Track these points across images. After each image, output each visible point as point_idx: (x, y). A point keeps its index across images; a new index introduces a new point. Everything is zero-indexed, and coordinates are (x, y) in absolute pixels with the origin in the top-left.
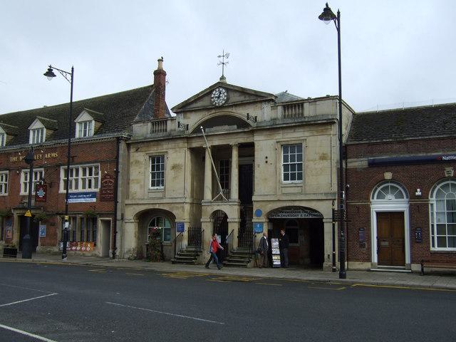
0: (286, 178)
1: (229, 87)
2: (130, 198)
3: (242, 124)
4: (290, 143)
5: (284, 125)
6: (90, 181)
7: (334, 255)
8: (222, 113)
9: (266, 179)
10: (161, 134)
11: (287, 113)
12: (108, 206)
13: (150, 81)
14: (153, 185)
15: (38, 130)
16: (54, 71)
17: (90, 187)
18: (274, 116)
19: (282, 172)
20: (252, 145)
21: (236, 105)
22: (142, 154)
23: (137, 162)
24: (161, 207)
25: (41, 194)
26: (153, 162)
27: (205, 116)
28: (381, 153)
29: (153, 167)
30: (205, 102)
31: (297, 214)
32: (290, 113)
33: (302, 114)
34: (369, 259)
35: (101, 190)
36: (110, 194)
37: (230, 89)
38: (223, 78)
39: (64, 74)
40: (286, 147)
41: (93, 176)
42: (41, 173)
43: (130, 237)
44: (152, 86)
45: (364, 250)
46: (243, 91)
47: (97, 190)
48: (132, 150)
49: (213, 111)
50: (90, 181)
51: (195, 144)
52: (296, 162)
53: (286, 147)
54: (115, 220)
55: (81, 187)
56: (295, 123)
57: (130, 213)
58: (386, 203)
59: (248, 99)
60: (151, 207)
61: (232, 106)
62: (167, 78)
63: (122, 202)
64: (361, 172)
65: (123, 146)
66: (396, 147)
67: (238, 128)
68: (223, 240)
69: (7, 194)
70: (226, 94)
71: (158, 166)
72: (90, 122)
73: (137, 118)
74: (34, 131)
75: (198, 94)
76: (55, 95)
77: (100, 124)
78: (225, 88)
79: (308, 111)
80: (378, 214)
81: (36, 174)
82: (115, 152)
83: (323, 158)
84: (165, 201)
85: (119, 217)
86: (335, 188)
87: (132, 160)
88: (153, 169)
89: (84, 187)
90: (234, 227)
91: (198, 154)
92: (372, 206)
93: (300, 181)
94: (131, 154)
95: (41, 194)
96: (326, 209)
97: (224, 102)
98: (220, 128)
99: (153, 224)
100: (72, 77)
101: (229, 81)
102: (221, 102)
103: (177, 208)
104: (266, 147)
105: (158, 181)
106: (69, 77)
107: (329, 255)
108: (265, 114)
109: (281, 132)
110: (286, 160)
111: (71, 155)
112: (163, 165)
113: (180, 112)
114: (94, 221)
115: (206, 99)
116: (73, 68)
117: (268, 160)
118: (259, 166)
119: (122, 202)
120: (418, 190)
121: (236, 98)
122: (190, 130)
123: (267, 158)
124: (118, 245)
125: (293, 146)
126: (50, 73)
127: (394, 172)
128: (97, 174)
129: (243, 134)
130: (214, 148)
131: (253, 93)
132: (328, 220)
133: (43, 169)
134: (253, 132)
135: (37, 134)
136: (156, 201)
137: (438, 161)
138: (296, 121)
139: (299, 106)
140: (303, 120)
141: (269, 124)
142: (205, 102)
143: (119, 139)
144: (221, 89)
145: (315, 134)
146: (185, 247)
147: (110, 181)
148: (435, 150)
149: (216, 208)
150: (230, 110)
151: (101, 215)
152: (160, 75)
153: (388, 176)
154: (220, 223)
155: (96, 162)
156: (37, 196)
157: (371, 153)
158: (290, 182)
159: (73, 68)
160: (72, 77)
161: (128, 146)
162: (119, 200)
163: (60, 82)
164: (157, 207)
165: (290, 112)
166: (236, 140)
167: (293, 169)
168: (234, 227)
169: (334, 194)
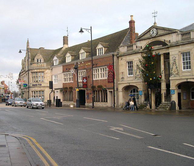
0: (184, 68)
1: (158, 28)
3: (164, 44)
4: (185, 52)
5: (182, 44)
6: (104, 74)
8: (156, 40)
10: (130, 52)
11: (183, 38)
12: (111, 85)
13: (127, 26)
14: (129, 75)
15: (83, 53)
16: (83, 30)
17: (104, 77)
18: (178, 40)
19: (183, 66)
20: (169, 53)
23: (122, 65)
24: (133, 84)
25: (85, 81)
26: (129, 64)
27: (150, 41)
29: (129, 66)
30: (147, 36)
32: (185, 38)
35: (108, 78)
36: (112, 79)
37: (158, 28)
38: (155, 23)
39: (88, 30)
40: (183, 54)
41: (105, 72)
42: (85, 72)
43: (121, 98)
44: (129, 28)
46: (163, 29)
47: (107, 78)
48: (120, 59)
49: (152, 39)
50: (104, 74)
52: (185, 61)
53: (183, 54)
54: (114, 91)
55: (100, 75)
57: (121, 88)
59: (166, 32)
61: (159, 36)
62: (135, 23)
63: (117, 83)
65: (115, 58)
69: (73, 82)
70: (156, 31)
71: (131, 66)
72: (84, 53)
73: (121, 45)
74: (81, 53)
75: (145, 32)
76: (85, 38)
77: (107, 49)
81: (94, 70)
82: (112, 61)
85: (115, 89)
87: (120, 64)
88: (129, 68)
89: (101, 77)
93: (190, 70)
94: (119, 61)
95: (85, 81)
97: (155, 35)
99: (131, 92)
100: (91, 31)
101: (158, 25)
102: (154, 35)
105: (131, 73)
106: (90, 31)
108: (173, 39)
109: (180, 46)
110: (184, 60)
111: (93, 64)
113: (138, 41)
114: (106, 91)
115: (148, 33)
116: (91, 27)
119: (117, 83)
121: (161, 32)
122: (143, 48)
124: (116, 102)
125: (186, 53)
126: (81, 31)
128: (106, 71)
131: (168, 29)
133: (85, 70)
134: (168, 48)
135: (83, 55)
138: (187, 41)
140: (190, 40)
142: (147, 36)
143: (113, 55)
144: (154, 29)
146: (142, 102)
150: (158, 38)
151: (109, 89)
152: (132, 23)
155: (105, 66)
156: (83, 82)
158: (186, 70)
159: (91, 27)
160: (91, 31)
161: (118, 57)
163: (86, 34)
166: (162, 52)
167: (187, 64)
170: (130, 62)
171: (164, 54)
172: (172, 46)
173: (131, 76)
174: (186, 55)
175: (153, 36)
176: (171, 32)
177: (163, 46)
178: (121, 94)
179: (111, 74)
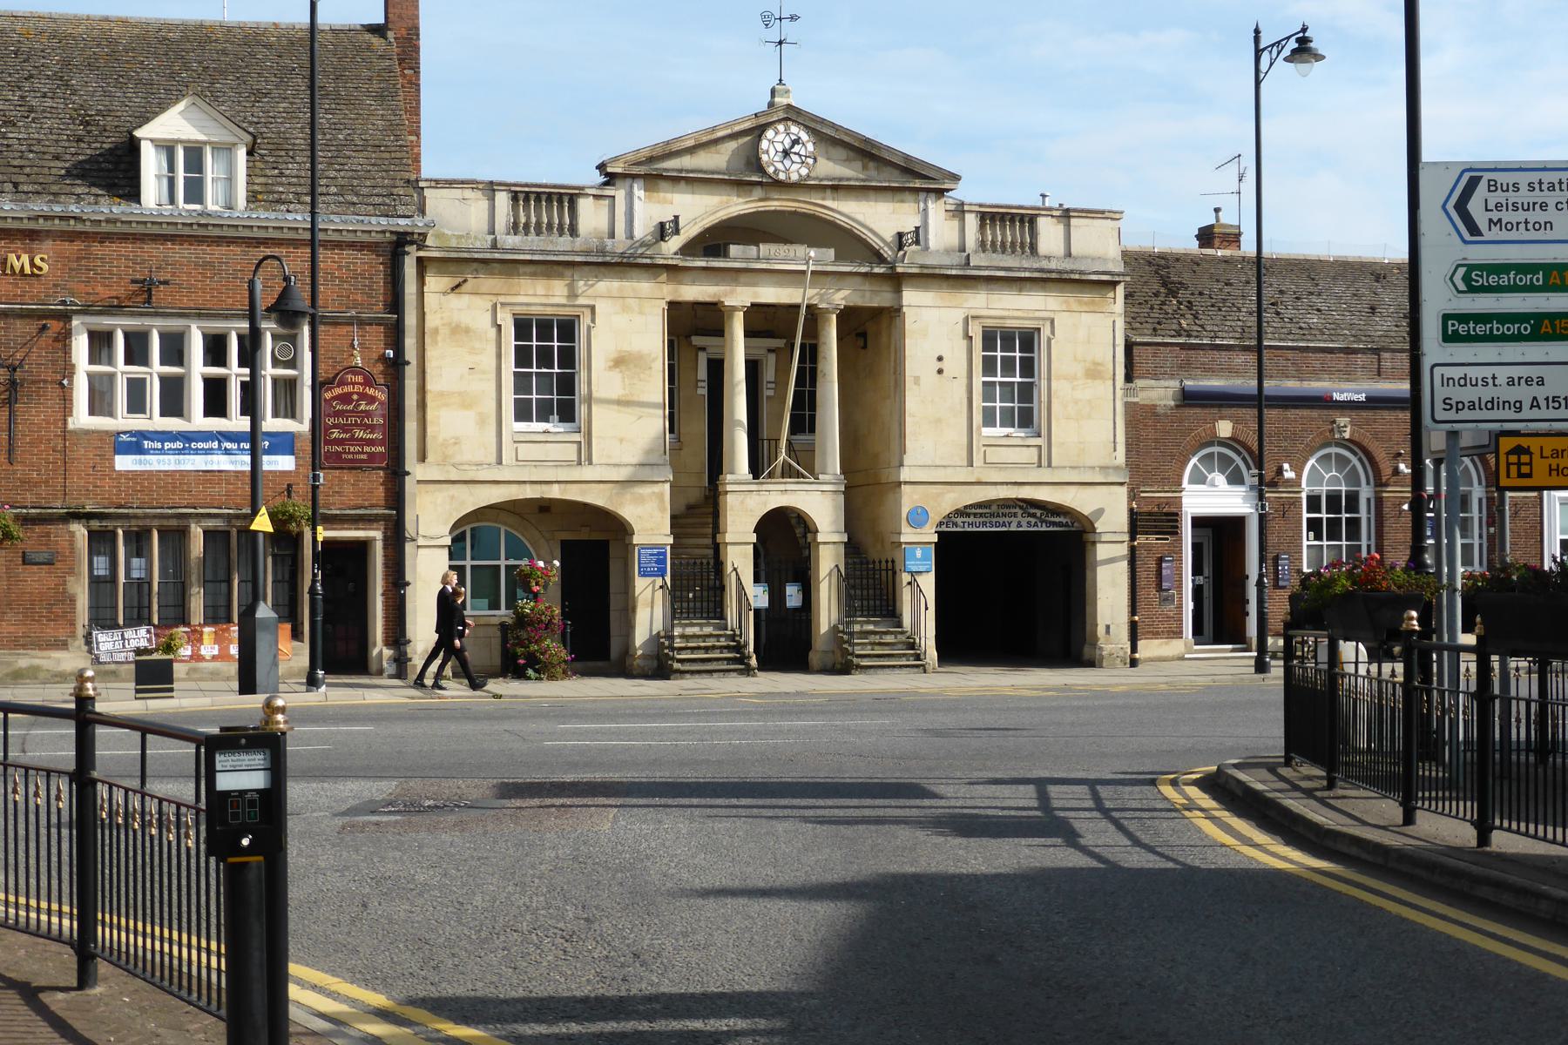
1: (818, 127)
2: (430, 457)
3: (849, 242)
7: (1133, 627)
9: (939, 421)
20: (893, 314)
21: (838, 188)
22: (485, 303)
23: (459, 331)
24: (574, 494)
27: (736, 205)
28: (1209, 370)
31: (1007, 519)
33: (1033, 248)
34: (1178, 634)
36: (371, 442)
37: (830, 137)
45: (1169, 609)
46: (865, 151)
48: (434, 283)
51: (692, 292)
56: (1025, 269)
58: (1212, 495)
61: (821, 188)
64: (1166, 415)
67: (839, 258)
68: (777, 596)
75: (714, 129)
78: (808, 128)
79: (1049, 236)
80: (1198, 522)
83: (1093, 373)
84: (587, 473)
86: (1120, 457)
90: (828, 561)
91: (692, 328)
92: (1184, 500)
96: (1109, 511)
97: (804, 171)
102: (795, 171)
107: (1108, 627)
112: (568, 358)
117: (944, 365)
118: (917, 380)
120: (1286, 466)
122: (673, 244)
123: (940, 359)
127: (1236, 421)
129: (858, 279)
136: (563, 475)
137: (1322, 402)
139: (1022, 221)
140: (1044, 264)
141: (946, 261)
144: (794, 129)
145: (1075, 307)
147: (363, 396)
148: (1316, 374)
153: (1225, 429)
154: (783, 539)
157: (1186, 367)
162: (411, 462)
164: (555, 492)
165: (997, 234)
168: (828, 561)
169: (1117, 468)
170: (545, 327)
172: (930, 278)
173: (542, 426)
174: (1009, 346)
175: (782, 176)
176: (917, 179)
177: (839, 258)
179: (372, 400)
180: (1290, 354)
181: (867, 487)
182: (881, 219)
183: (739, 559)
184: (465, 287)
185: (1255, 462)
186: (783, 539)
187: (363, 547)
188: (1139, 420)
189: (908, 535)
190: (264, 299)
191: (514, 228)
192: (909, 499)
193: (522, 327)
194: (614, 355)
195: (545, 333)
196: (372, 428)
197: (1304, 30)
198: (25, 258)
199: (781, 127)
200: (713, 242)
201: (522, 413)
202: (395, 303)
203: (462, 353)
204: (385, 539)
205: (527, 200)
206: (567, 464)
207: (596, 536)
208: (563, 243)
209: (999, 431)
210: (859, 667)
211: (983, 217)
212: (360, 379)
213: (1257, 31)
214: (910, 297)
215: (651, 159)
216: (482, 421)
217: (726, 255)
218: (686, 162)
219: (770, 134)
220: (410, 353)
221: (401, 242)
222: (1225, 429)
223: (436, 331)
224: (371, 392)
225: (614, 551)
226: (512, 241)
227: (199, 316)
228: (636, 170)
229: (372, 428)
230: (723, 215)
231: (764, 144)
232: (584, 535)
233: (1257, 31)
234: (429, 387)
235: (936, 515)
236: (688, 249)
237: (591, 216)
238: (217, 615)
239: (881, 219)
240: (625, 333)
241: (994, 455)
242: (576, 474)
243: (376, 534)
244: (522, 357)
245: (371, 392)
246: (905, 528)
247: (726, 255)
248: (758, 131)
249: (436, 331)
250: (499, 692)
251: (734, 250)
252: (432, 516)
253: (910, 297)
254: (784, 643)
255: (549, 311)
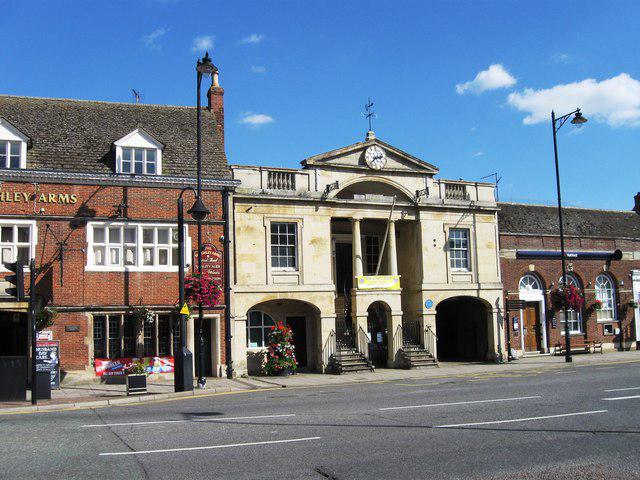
0: (452, 266)
3: (401, 195)
20: (417, 222)
23: (250, 229)
24: (296, 297)
27: (357, 178)
28: (525, 246)
34: (520, 348)
36: (215, 276)
51: (341, 213)
57: (240, 307)
59: (406, 167)
60: (279, 297)
66: (535, 241)
79: (470, 190)
83: (489, 247)
90: (397, 322)
91: (340, 226)
97: (382, 166)
98: (374, 197)
102: (377, 165)
103: (323, 299)
104: (433, 230)
112: (293, 240)
118: (427, 250)
122: (333, 194)
130: (365, 222)
132: (362, 314)
144: (378, 149)
147: (211, 256)
149: (375, 298)
150: (390, 177)
154: (379, 312)
164: (289, 296)
168: (397, 322)
171: (400, 224)
173: (284, 268)
177: (397, 200)
178: (239, 330)
179: (215, 257)
180: (552, 240)
181: (411, 289)
182: (410, 185)
183: (362, 323)
184: (252, 210)
185: (539, 281)
186: (379, 312)
187: (214, 319)
188: (505, 264)
189: (425, 311)
190: (187, 208)
191: (269, 186)
192: (426, 296)
193: (274, 227)
194: (311, 239)
195: (283, 230)
196: (216, 270)
197: (578, 110)
198: (67, 196)
199: (373, 148)
200: (348, 193)
201: (275, 264)
202: (225, 217)
203: (250, 235)
204: (221, 317)
205: (279, 175)
206: (294, 284)
207: (301, 315)
208: (290, 192)
209: (455, 269)
210: (414, 366)
211: (447, 185)
212: (210, 248)
213: (553, 113)
214: (423, 215)
215: (324, 160)
216: (259, 267)
217: (352, 198)
218: (337, 161)
219: (369, 150)
220: (231, 238)
221: (225, 192)
222: (532, 268)
223: (239, 229)
224: (215, 254)
225: (308, 321)
226: (269, 191)
227: (142, 221)
228: (318, 163)
229: (216, 270)
230: (352, 182)
231: (367, 154)
232: (296, 314)
233: (553, 113)
234: (237, 252)
235: (436, 303)
236: (339, 196)
237: (301, 182)
238: (165, 354)
239: (410, 185)
240: (315, 230)
241: (456, 278)
242: (297, 288)
243: (218, 316)
244: (274, 240)
245: (215, 254)
246: (424, 309)
247: (352, 198)
248: (364, 149)
249: (239, 229)
250: (284, 384)
251: (356, 196)
252: (240, 307)
253: (423, 215)
254: (380, 357)
255: (286, 220)
